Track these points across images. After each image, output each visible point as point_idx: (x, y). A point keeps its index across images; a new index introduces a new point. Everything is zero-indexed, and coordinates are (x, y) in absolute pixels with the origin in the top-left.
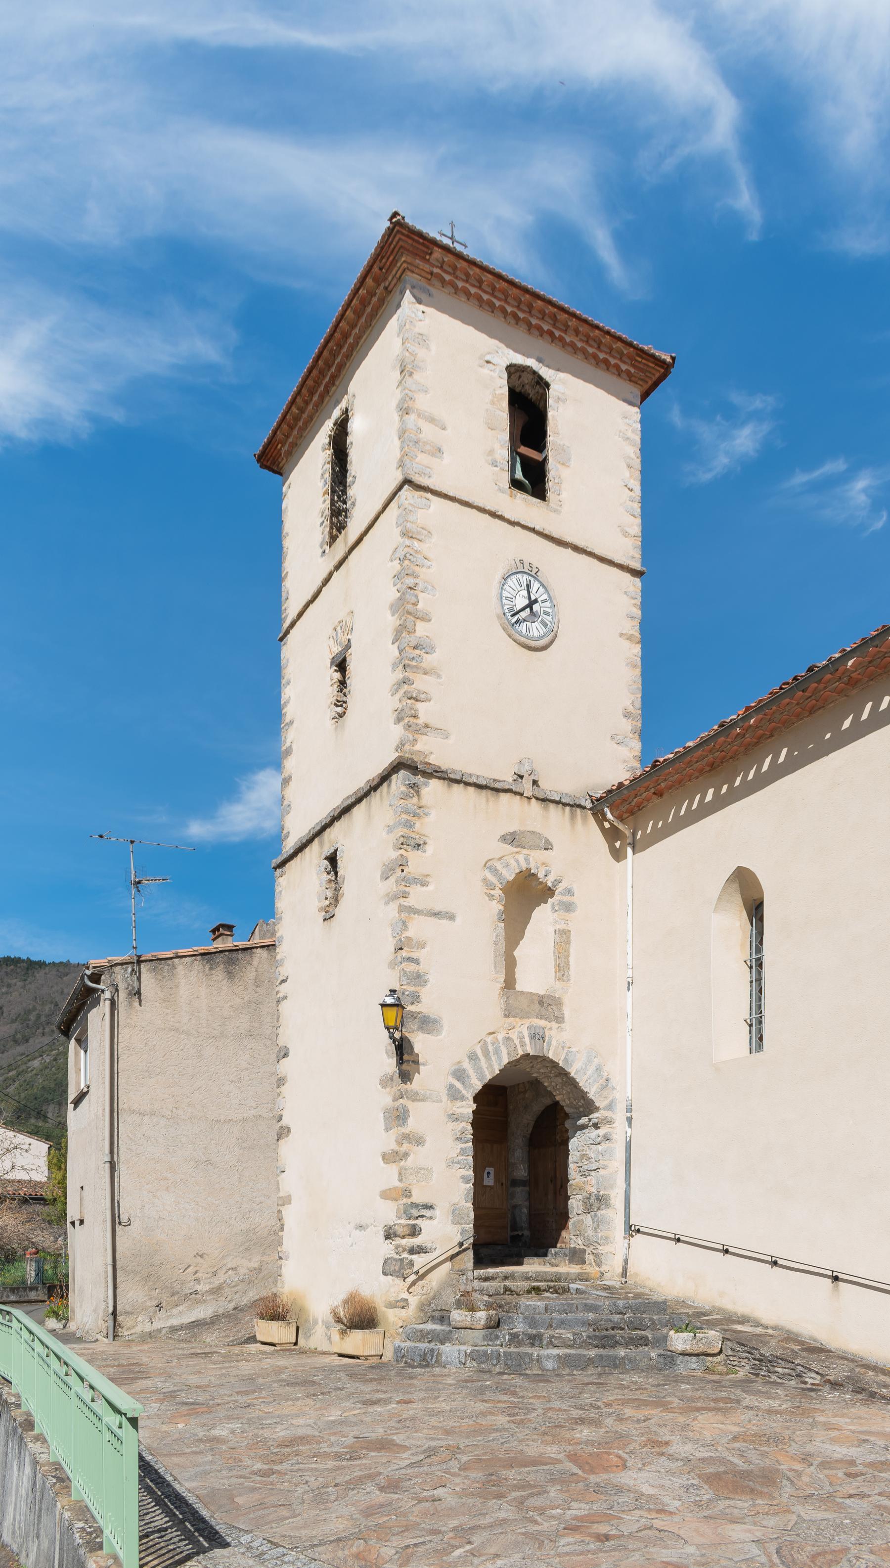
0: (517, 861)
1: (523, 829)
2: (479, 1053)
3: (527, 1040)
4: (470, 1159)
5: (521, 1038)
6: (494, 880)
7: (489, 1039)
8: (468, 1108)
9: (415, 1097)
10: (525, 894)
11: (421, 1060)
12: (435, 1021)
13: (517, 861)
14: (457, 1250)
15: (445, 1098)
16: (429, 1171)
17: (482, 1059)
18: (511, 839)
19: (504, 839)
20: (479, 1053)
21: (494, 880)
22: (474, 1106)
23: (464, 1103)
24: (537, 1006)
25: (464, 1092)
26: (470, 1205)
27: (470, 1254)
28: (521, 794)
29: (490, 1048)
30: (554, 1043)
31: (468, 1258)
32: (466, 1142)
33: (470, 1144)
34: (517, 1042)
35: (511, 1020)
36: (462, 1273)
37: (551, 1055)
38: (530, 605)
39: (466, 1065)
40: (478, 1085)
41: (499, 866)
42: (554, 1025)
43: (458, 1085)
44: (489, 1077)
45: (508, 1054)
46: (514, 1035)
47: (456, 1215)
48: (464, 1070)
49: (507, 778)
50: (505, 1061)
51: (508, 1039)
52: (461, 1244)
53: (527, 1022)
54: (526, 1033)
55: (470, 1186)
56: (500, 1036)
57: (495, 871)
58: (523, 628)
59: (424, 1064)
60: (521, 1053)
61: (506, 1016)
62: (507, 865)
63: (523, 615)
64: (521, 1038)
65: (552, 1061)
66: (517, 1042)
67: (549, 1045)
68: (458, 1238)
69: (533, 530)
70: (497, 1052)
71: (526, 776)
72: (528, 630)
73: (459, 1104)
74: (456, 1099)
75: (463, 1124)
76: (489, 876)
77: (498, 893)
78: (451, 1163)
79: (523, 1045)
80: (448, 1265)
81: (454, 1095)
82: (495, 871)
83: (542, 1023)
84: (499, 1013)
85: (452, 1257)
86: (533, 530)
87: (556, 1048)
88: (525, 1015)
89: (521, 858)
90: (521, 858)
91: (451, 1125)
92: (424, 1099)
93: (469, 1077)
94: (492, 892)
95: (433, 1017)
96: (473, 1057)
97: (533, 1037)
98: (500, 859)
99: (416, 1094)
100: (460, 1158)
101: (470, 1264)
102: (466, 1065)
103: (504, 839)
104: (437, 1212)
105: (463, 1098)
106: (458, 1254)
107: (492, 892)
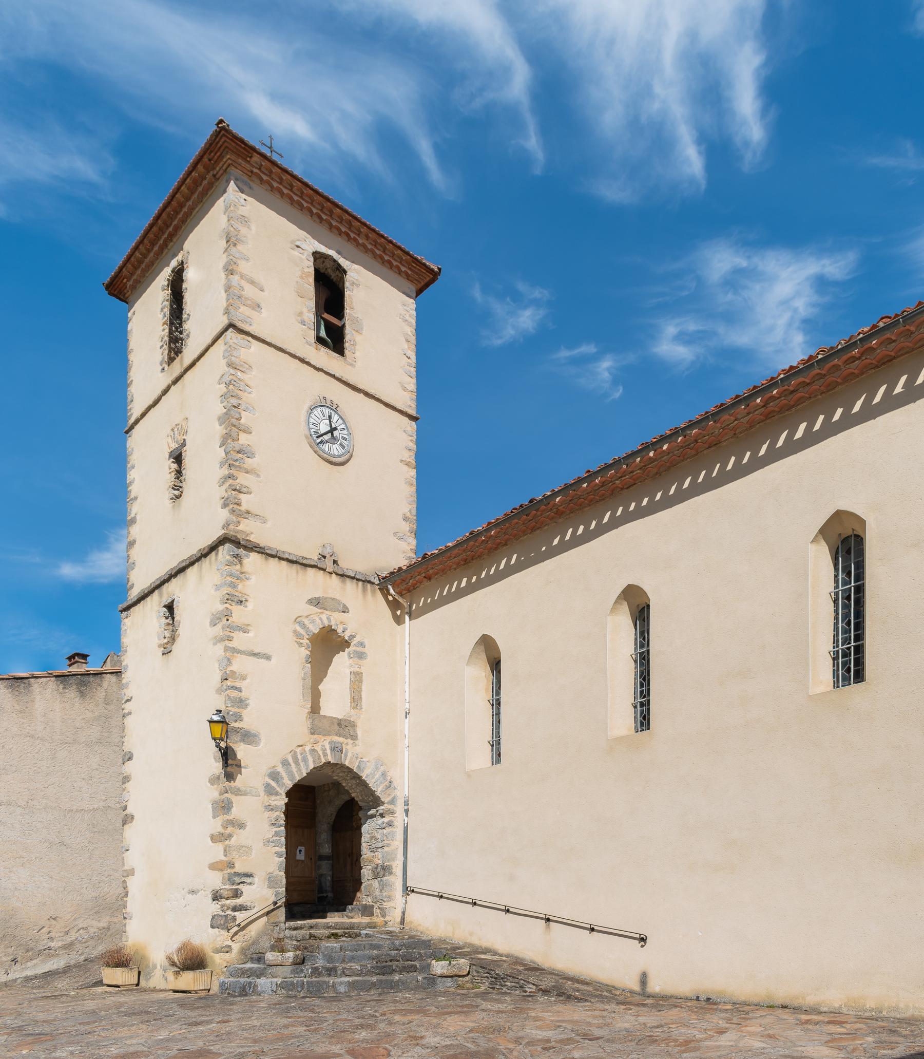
0: (321, 619)
1: (325, 596)
2: (290, 760)
3: (328, 751)
4: (283, 839)
5: (324, 750)
6: (302, 632)
7: (299, 750)
8: (282, 801)
9: (238, 792)
10: (327, 645)
11: (243, 765)
12: (255, 736)
13: (321, 619)
14: (272, 907)
15: (262, 793)
16: (249, 848)
17: (293, 765)
18: (316, 602)
19: (310, 602)
20: (290, 760)
21: (302, 632)
22: (286, 800)
23: (278, 797)
24: (337, 727)
25: (278, 789)
26: (282, 874)
27: (283, 911)
28: (324, 570)
29: (299, 757)
30: (350, 755)
31: (281, 913)
32: (280, 827)
33: (283, 828)
34: (320, 753)
35: (316, 736)
36: (276, 924)
37: (347, 763)
38: (332, 430)
39: (280, 769)
40: (290, 785)
41: (306, 622)
42: (350, 741)
43: (273, 784)
44: (298, 778)
45: (314, 761)
46: (318, 748)
47: (271, 881)
48: (278, 773)
49: (314, 557)
50: (311, 766)
51: (314, 750)
52: (275, 903)
53: (329, 739)
54: (328, 747)
55: (283, 859)
56: (307, 748)
57: (303, 626)
58: (326, 447)
59: (245, 768)
60: (323, 761)
61: (312, 734)
62: (313, 622)
63: (326, 437)
64: (324, 750)
65: (348, 768)
66: (320, 753)
67: (346, 756)
68: (273, 899)
69: (333, 376)
70: (305, 760)
71: (328, 556)
72: (330, 449)
73: (274, 798)
74: (272, 794)
75: (278, 813)
76: (299, 629)
77: (305, 641)
78: (267, 842)
79: (325, 755)
80: (265, 919)
81: (270, 791)
82: (303, 626)
83: (341, 739)
84: (307, 731)
85: (268, 913)
86: (333, 376)
87: (352, 758)
88: (327, 733)
89: (324, 617)
90: (324, 617)
91: (267, 814)
92: (245, 794)
93: (282, 778)
94: (301, 641)
95: (252, 731)
96: (285, 763)
97: (333, 749)
98: (307, 617)
99: (239, 790)
100: (275, 838)
101: (282, 917)
102: (280, 769)
103: (310, 602)
104: (256, 880)
105: (277, 794)
106: (273, 910)
107: (301, 641)
